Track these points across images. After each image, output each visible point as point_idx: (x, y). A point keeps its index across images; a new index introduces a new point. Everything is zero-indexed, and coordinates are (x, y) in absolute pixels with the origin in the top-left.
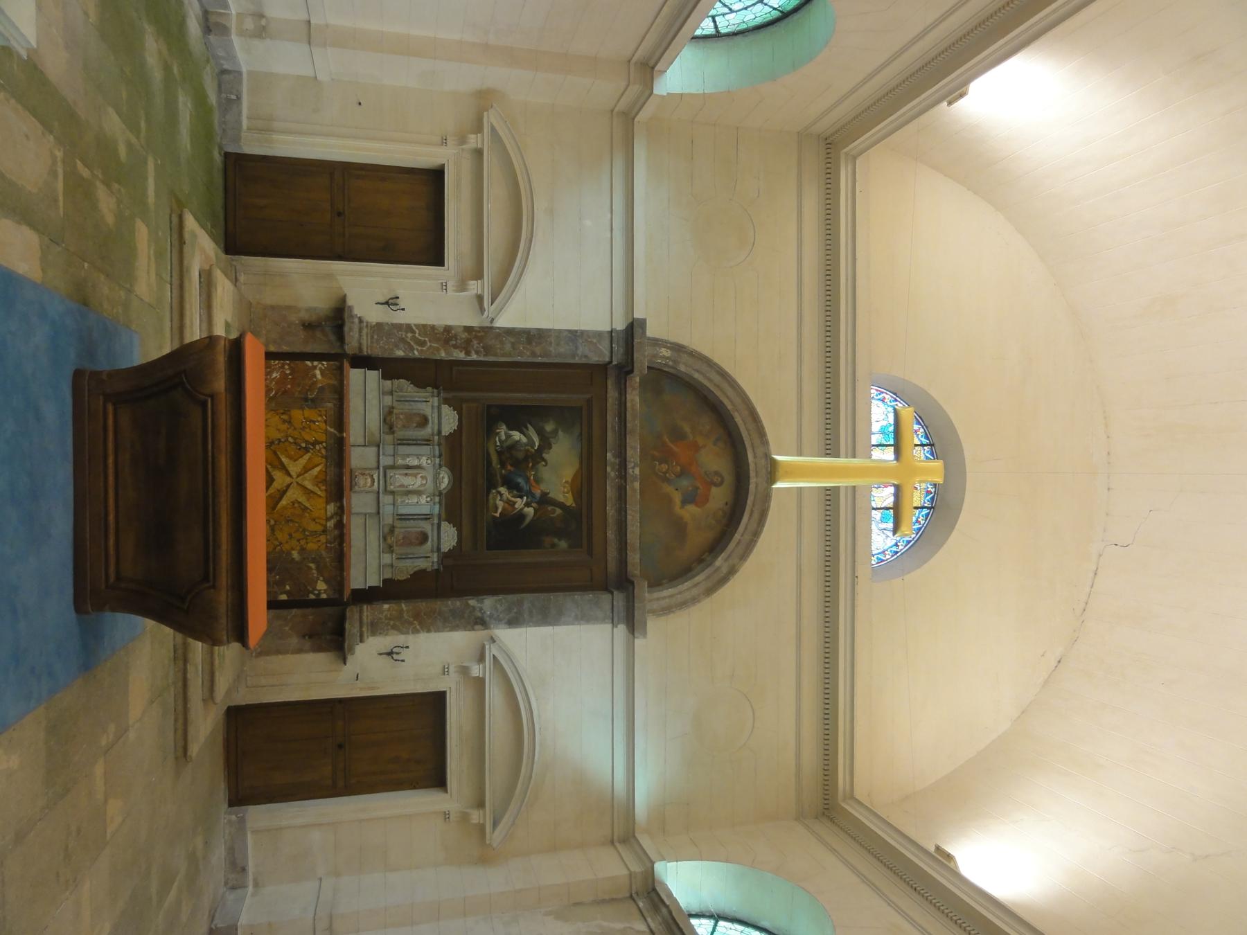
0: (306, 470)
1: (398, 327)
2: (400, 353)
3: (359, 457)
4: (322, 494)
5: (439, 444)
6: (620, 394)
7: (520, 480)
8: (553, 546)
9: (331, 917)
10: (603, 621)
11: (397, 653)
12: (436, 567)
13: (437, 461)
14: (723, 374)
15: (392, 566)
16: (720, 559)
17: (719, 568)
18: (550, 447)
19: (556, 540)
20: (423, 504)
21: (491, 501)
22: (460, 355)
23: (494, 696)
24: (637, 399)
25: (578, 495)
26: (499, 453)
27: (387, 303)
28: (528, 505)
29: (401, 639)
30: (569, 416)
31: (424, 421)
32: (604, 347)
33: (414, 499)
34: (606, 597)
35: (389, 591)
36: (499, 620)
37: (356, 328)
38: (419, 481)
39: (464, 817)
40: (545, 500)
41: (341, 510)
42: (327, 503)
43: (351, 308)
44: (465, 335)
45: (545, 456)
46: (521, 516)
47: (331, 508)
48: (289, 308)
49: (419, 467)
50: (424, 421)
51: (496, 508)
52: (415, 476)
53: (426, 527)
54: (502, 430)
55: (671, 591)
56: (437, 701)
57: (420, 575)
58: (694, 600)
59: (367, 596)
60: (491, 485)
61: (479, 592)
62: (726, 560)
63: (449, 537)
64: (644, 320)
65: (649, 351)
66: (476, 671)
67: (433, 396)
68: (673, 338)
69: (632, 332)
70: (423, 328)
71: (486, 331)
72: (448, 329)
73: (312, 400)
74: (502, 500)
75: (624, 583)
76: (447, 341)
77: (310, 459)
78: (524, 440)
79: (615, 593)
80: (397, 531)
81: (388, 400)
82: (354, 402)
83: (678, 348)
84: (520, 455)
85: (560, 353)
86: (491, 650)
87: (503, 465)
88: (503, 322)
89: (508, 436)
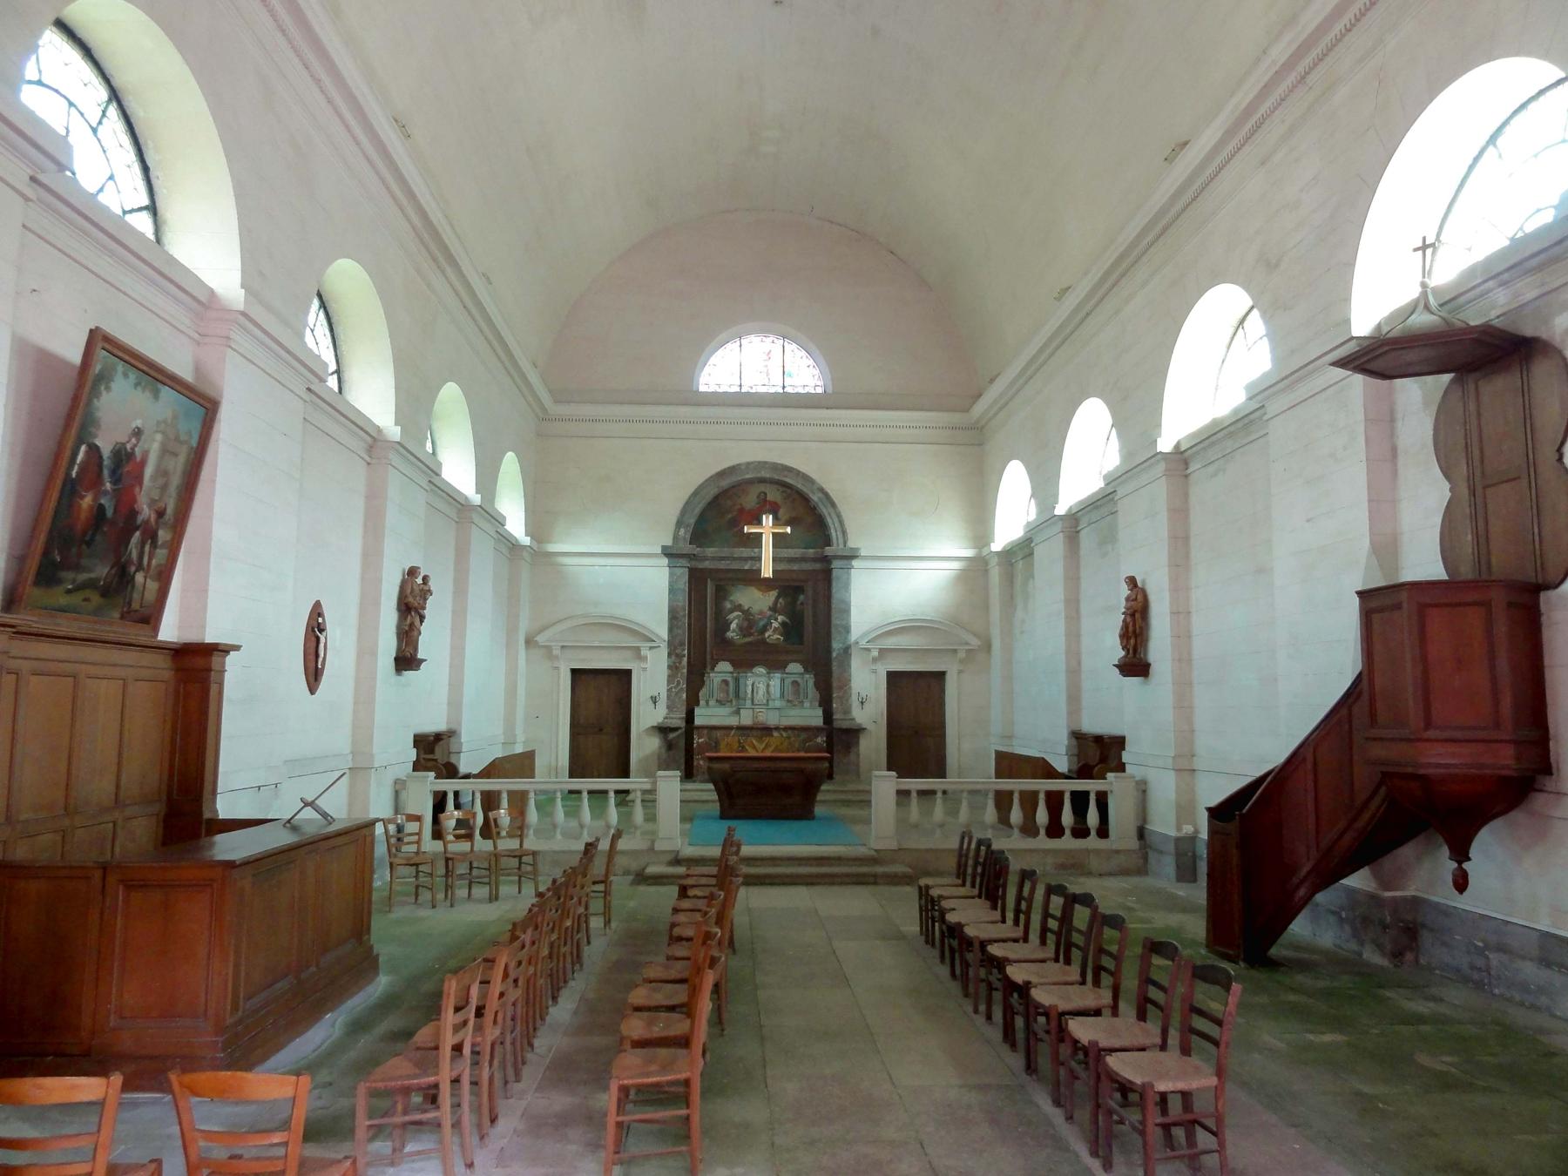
0: (754, 747)
1: (669, 697)
2: (684, 695)
3: (746, 719)
4: (768, 739)
5: (739, 673)
6: (707, 560)
7: (762, 623)
8: (802, 604)
9: (1003, 737)
10: (849, 574)
11: (863, 699)
12: (812, 676)
13: (750, 674)
14: (695, 493)
15: (811, 702)
16: (813, 498)
17: (819, 498)
18: (740, 605)
19: (799, 602)
20: (776, 680)
21: (775, 642)
22: (685, 659)
23: (891, 642)
24: (711, 549)
25: (773, 588)
26: (744, 636)
27: (655, 703)
28: (776, 619)
29: (854, 698)
30: (721, 593)
31: (726, 682)
32: (679, 571)
33: (772, 689)
34: (835, 573)
35: (826, 703)
36: (846, 638)
37: (669, 721)
38: (761, 685)
39: (961, 661)
40: (774, 609)
41: (777, 728)
42: (772, 736)
43: (659, 724)
44: (673, 657)
45: (746, 608)
46: (783, 624)
47: (776, 734)
48: (659, 759)
49: (753, 685)
50: (726, 682)
51: (778, 639)
52: (758, 688)
53: (788, 681)
54: (730, 634)
55: (833, 531)
56: (893, 677)
57: (817, 685)
58: (839, 516)
59: (828, 716)
60: (764, 642)
61: (829, 650)
62: (814, 493)
63: (795, 668)
64: (663, 546)
65: (681, 545)
66: (875, 653)
67: (709, 677)
68: (672, 527)
69: (668, 553)
70: (669, 682)
71: (670, 643)
72: (670, 667)
73: (716, 743)
74: (773, 636)
75: (826, 560)
76: (677, 668)
77: (749, 745)
78: (736, 621)
79: (833, 567)
80: (790, 699)
81: (712, 703)
82: (714, 722)
83: (679, 524)
84: (746, 624)
85: (683, 600)
86: (863, 644)
87: (751, 634)
88: (666, 638)
89: (734, 631)
